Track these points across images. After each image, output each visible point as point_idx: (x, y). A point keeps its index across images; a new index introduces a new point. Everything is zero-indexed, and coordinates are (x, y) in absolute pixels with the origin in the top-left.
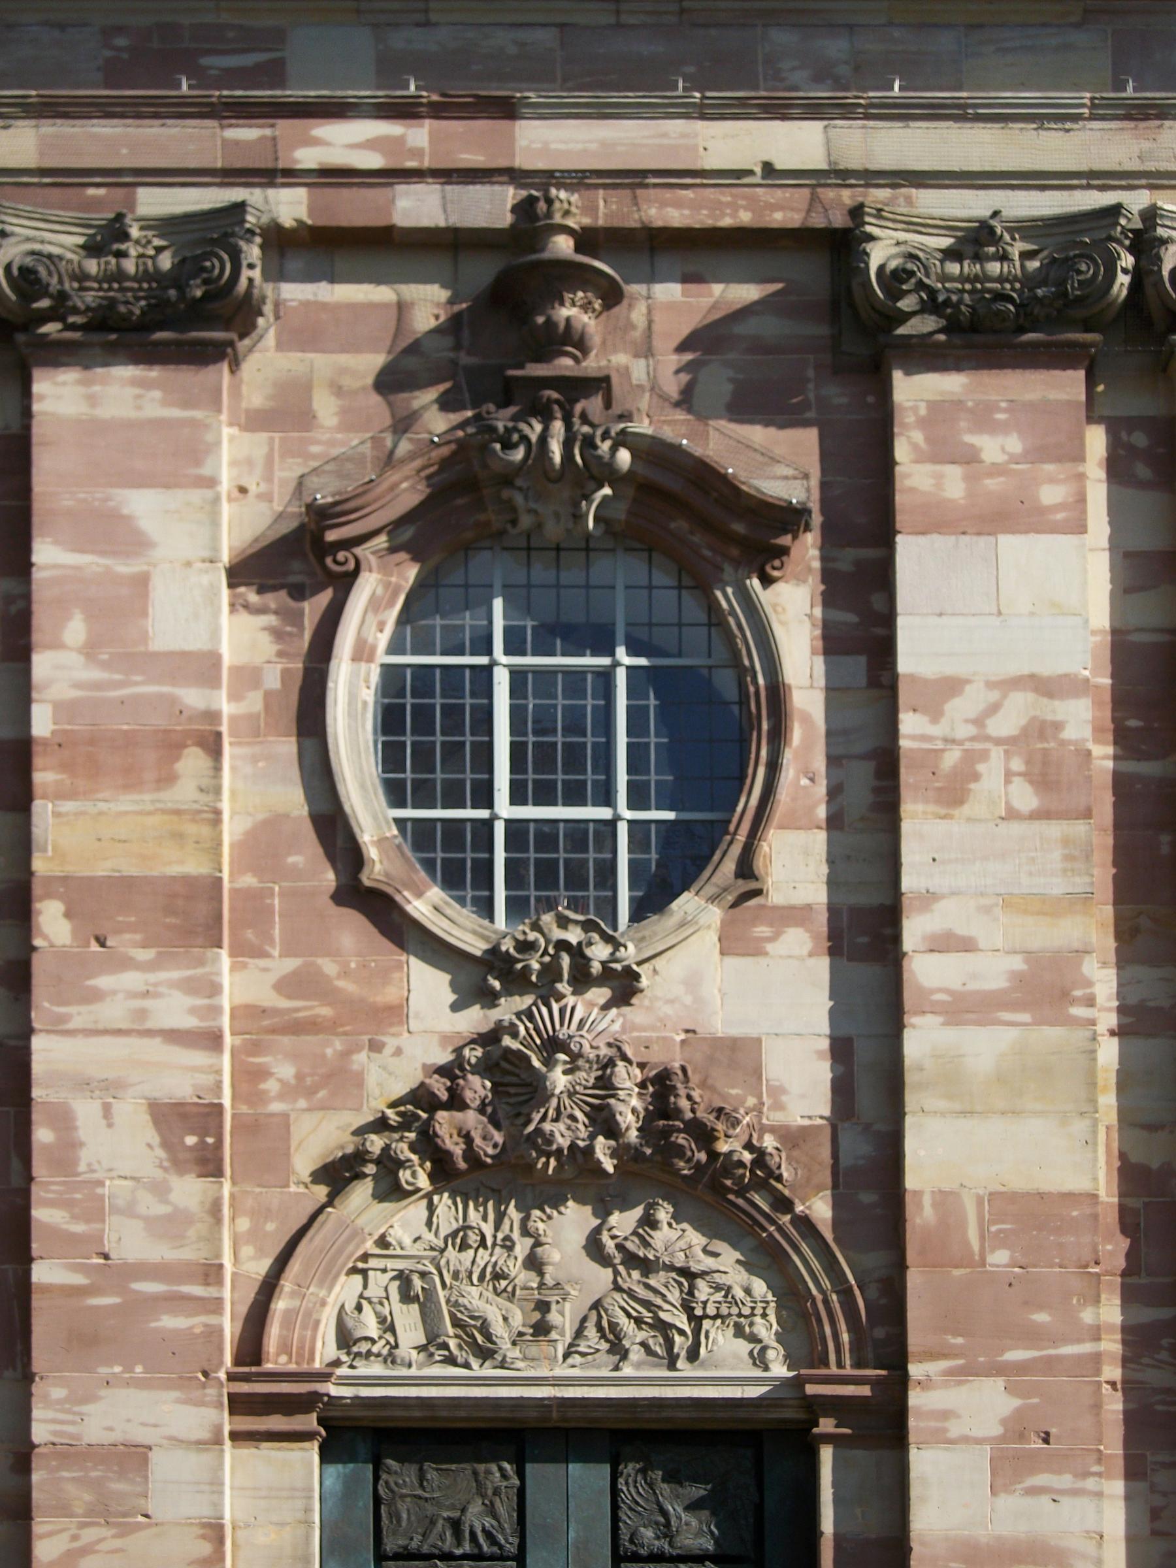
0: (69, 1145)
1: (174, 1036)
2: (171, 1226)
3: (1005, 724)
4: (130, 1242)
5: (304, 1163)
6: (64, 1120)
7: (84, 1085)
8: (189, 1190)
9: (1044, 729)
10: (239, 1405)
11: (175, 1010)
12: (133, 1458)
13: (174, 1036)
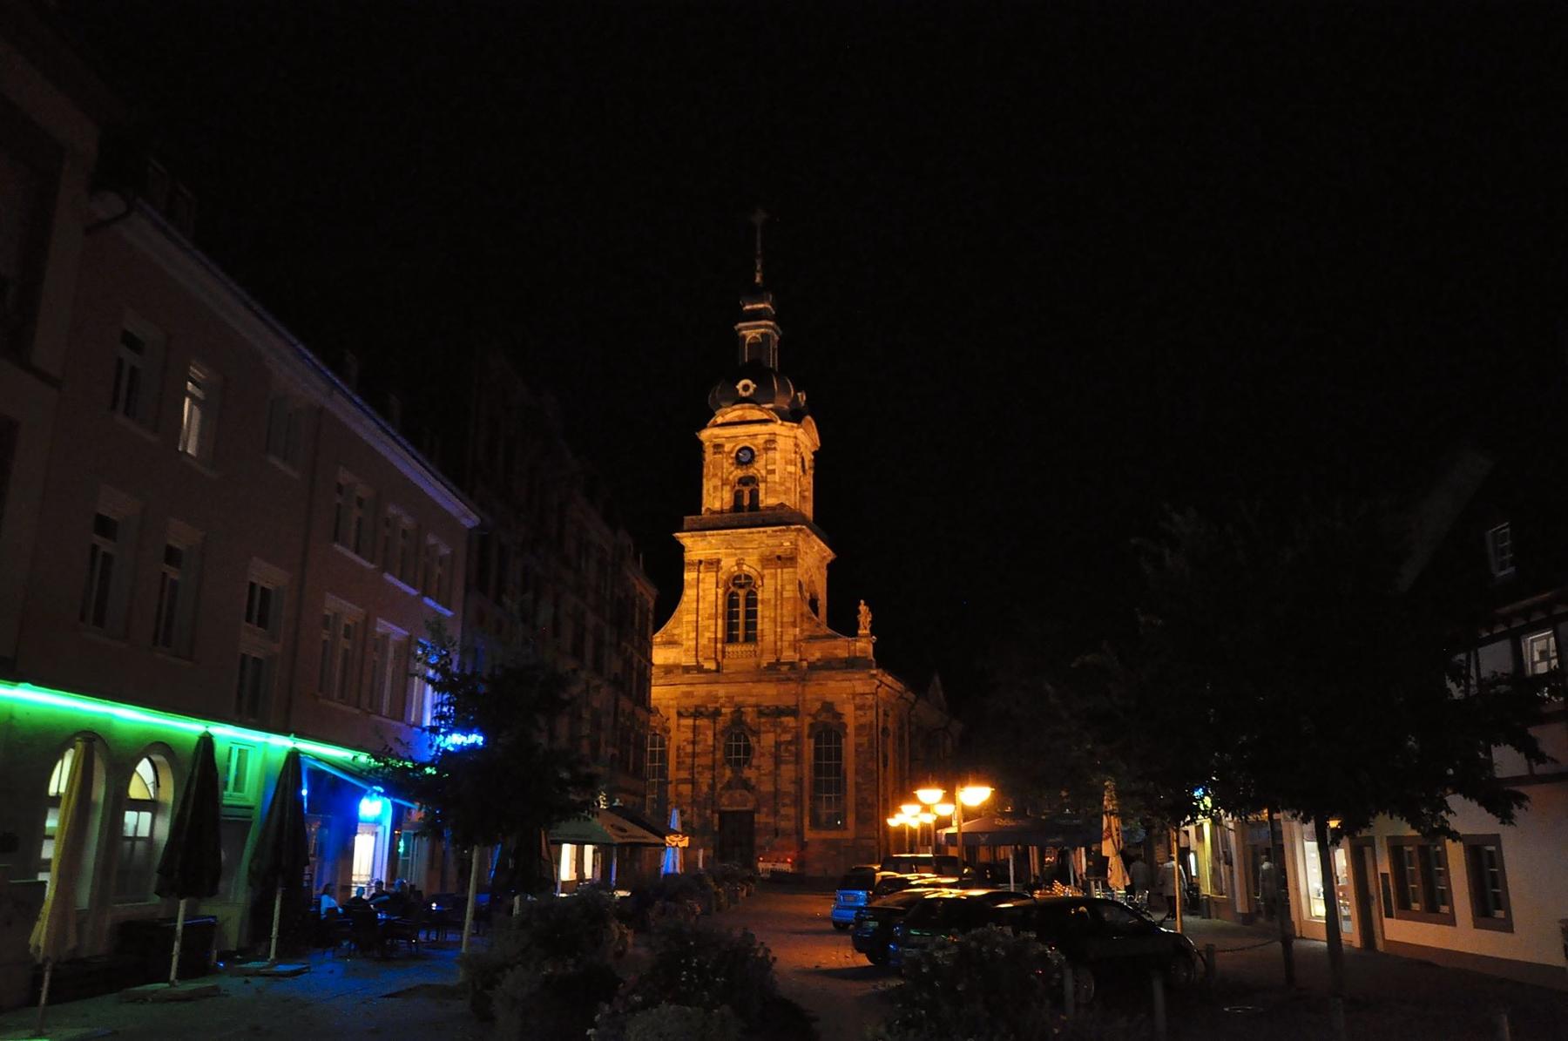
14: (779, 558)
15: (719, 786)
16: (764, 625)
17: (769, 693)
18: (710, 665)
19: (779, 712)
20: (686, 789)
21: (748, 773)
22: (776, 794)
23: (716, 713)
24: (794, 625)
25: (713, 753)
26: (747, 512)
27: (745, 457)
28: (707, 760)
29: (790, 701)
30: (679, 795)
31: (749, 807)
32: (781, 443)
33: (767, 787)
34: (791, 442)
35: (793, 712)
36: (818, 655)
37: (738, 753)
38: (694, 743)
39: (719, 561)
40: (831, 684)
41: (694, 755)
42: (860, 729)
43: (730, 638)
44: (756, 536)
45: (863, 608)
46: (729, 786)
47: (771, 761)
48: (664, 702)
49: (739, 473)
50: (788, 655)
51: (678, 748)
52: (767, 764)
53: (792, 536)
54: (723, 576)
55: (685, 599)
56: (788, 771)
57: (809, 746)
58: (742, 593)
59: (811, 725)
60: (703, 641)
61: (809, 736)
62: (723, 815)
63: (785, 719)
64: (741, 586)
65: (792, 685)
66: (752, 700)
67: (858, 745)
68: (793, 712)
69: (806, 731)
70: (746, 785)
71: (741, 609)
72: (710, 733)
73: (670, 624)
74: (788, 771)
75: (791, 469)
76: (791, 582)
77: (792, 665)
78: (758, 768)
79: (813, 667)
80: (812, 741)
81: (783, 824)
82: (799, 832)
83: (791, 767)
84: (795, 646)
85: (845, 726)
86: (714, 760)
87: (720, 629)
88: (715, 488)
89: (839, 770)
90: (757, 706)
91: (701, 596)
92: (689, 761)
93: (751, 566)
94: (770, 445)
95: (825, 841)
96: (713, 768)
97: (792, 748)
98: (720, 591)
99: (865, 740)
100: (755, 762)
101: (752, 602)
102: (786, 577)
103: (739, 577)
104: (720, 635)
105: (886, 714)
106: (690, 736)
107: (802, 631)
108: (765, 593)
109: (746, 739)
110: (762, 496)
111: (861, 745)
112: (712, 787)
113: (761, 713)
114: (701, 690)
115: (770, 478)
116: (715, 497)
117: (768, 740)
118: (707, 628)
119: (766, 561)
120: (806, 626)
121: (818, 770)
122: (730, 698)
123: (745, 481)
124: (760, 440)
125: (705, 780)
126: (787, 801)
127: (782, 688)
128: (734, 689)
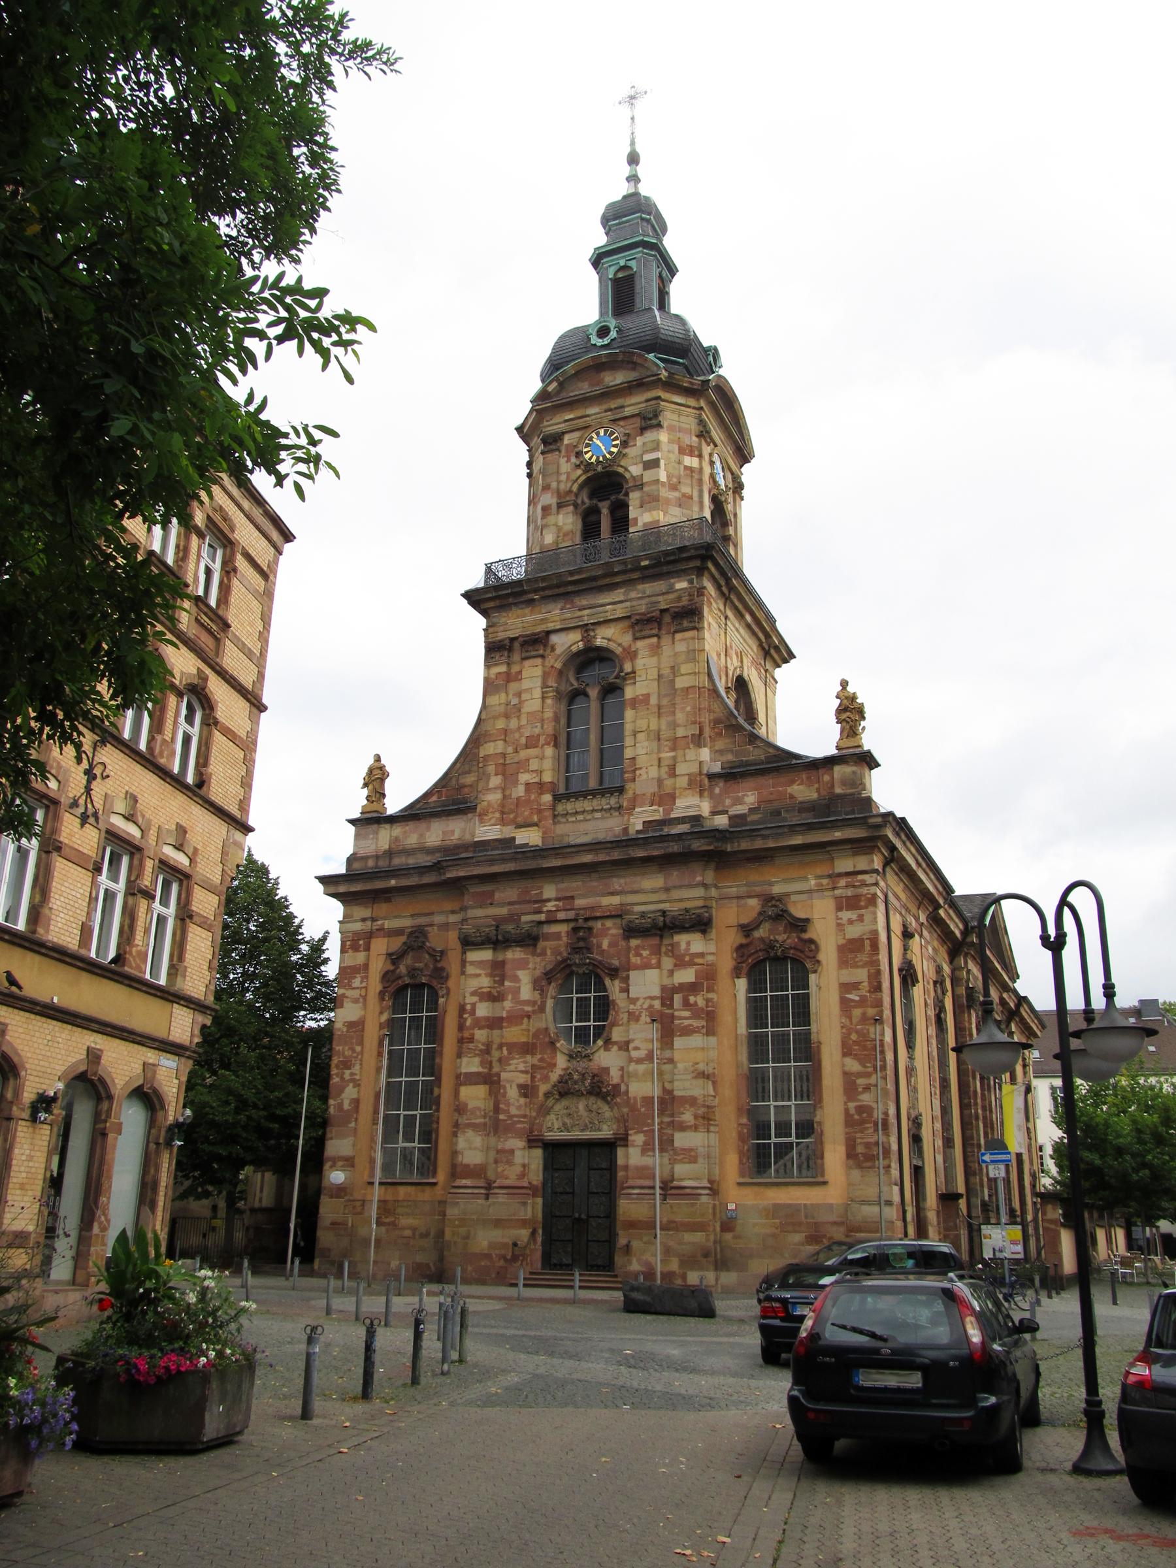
0: (505, 1093)
1: (522, 1072)
2: (519, 1108)
3: (645, 1006)
4: (513, 1111)
5: (541, 1094)
6: (505, 1087)
7: (508, 1081)
8: (522, 1100)
9: (651, 1006)
10: (529, 1141)
11: (521, 1067)
12: (512, 1152)
13: (522, 1072)
20: (475, 1096)
21: (607, 1059)
22: (669, 1101)
31: (606, 1132)
35: (701, 924)
36: (751, 799)
46: (565, 1090)
47: (654, 1031)
51: (462, 1009)
52: (643, 1035)
57: (737, 993)
61: (737, 972)
63: (682, 939)
67: (846, 987)
69: (726, 963)
70: (600, 1089)
78: (625, 1046)
80: (742, 984)
81: (687, 1174)
82: (714, 1190)
88: (546, 509)
89: (808, 1050)
95: (776, 1210)
97: (699, 1000)
99: (861, 975)
100: (617, 1034)
105: (907, 935)
109: (601, 986)
110: (633, 513)
111: (854, 986)
112: (527, 1091)
113: (631, 931)
115: (648, 476)
121: (757, 1047)
125: (514, 1074)
126: (688, 1117)
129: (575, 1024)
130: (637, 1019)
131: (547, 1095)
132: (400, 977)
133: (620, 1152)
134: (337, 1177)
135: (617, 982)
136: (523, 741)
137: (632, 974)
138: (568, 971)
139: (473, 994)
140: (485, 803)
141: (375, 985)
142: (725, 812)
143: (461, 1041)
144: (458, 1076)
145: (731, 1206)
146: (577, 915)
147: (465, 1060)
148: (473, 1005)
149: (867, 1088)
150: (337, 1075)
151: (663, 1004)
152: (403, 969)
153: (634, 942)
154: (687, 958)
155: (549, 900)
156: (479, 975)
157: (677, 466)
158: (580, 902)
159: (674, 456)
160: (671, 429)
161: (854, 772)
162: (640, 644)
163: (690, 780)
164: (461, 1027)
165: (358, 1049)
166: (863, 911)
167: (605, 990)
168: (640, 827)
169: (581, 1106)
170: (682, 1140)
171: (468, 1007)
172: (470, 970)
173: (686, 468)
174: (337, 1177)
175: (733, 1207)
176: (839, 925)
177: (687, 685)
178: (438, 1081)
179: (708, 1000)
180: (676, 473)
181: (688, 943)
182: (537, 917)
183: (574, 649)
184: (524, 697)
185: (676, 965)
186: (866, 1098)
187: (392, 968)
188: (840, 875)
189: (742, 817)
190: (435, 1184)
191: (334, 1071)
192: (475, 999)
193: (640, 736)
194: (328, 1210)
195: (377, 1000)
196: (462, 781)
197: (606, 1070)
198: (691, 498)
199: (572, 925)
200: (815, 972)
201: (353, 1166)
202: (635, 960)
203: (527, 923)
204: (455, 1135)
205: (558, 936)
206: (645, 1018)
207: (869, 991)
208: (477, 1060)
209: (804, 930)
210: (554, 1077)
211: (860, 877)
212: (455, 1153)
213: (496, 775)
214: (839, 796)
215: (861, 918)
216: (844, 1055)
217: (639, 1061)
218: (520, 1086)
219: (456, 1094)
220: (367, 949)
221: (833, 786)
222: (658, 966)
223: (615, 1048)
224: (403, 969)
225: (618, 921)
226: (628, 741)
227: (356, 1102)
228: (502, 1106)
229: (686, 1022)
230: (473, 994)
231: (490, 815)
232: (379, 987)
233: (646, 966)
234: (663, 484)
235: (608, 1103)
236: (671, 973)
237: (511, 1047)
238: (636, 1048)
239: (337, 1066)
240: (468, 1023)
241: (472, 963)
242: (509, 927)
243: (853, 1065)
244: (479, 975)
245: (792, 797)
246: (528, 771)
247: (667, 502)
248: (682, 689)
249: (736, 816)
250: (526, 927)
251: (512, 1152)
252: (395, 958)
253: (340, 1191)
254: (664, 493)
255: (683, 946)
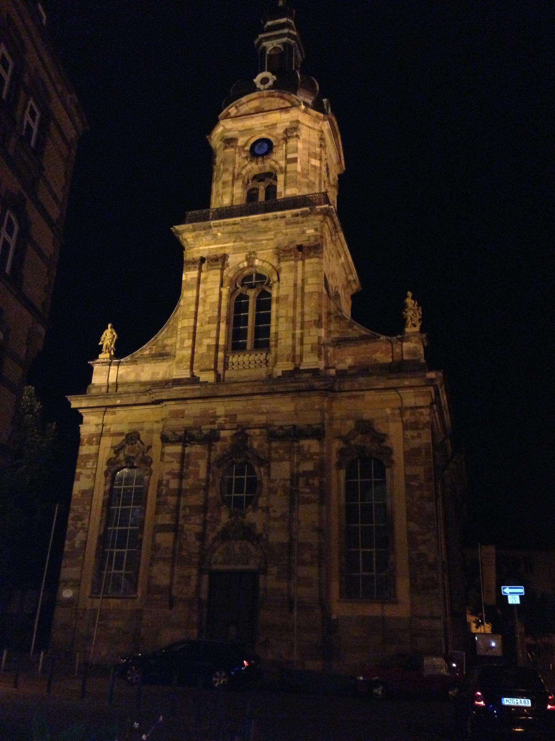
9: (284, 485)
11: (198, 521)
14: (300, 248)
15: (211, 536)
16: (280, 326)
17: (283, 409)
18: (208, 377)
19: (295, 434)
20: (165, 539)
23: (211, 438)
24: (318, 324)
25: (206, 489)
26: (262, 198)
27: (262, 148)
28: (196, 500)
29: (311, 418)
30: (155, 547)
31: (252, 566)
32: (304, 132)
33: (278, 537)
34: (314, 137)
36: (349, 361)
37: (239, 489)
38: (181, 476)
39: (224, 257)
40: (370, 396)
41: (179, 492)
42: (411, 455)
43: (236, 344)
44: (271, 224)
45: (409, 301)
48: (147, 426)
49: (254, 167)
50: (310, 361)
51: (160, 484)
52: (279, 503)
53: (317, 220)
54: (229, 273)
55: (182, 303)
56: (308, 514)
57: (338, 478)
58: (252, 294)
59: (341, 452)
60: (201, 350)
61: (339, 466)
62: (214, 575)
63: (305, 443)
64: (251, 287)
65: (316, 399)
66: (263, 419)
67: (409, 478)
68: (317, 433)
69: (334, 459)
71: (251, 314)
72: (203, 464)
73: (162, 334)
74: (308, 514)
75: (315, 162)
76: (315, 274)
77: (315, 372)
78: (267, 510)
79: (342, 374)
80: (343, 473)
82: (324, 604)
83: (314, 507)
84: (319, 349)
85: (389, 451)
86: (207, 501)
87: (222, 334)
90: (266, 426)
91: (202, 297)
92: (172, 500)
93: (264, 261)
94: (291, 132)
96: (204, 509)
98: (225, 291)
99: (419, 470)
100: (262, 502)
101: (264, 303)
102: (308, 268)
103: (249, 277)
104: (222, 342)
106: (176, 466)
107: (329, 333)
108: (281, 289)
109: (252, 471)
110: (280, 188)
111: (415, 477)
112: (202, 537)
114: (194, 408)
115: (290, 167)
116: (226, 192)
117: (281, 470)
118: (206, 334)
119: (282, 253)
120: (333, 327)
121: (350, 513)
122: (231, 417)
123: (259, 178)
124: (280, 131)
125: (192, 526)
126: (307, 557)
127: (302, 402)
128: (236, 405)
129: (233, 495)
130: (275, 493)
131: (215, 539)
132: (119, 462)
133: (261, 578)
134: (67, 594)
135: (262, 469)
136: (207, 319)
137: (273, 464)
138: (230, 461)
139: (167, 474)
140: (181, 356)
141: (102, 466)
142: (334, 367)
143: (158, 504)
144: (155, 527)
145: (334, 617)
146: (238, 426)
147: (160, 517)
148: (168, 481)
149: (424, 542)
150: (72, 525)
151: (292, 484)
152: (121, 456)
153: (274, 445)
154: (308, 456)
155: (220, 417)
156: (172, 462)
157: (307, 164)
158: (240, 418)
159: (306, 158)
160: (304, 141)
161: (416, 347)
162: (283, 265)
163: (312, 347)
164: (159, 495)
165: (88, 508)
166: (421, 432)
167: (254, 473)
168: (280, 374)
169: (237, 548)
170: (303, 571)
171: (165, 482)
172: (167, 458)
173: (312, 165)
174: (67, 594)
175: (336, 617)
176: (405, 439)
177: (312, 290)
178: (141, 530)
179: (321, 483)
180: (306, 167)
181: (309, 446)
182: (212, 426)
183: (241, 266)
184: (208, 293)
185: (301, 460)
186: (423, 548)
187: (114, 456)
188: (406, 408)
189: (345, 371)
190: (135, 598)
191: (70, 522)
192: (169, 477)
193: (281, 320)
194: (60, 615)
195: (103, 477)
196: (166, 342)
197: (254, 525)
198: (314, 183)
199: (234, 432)
200: (390, 467)
201: (79, 585)
202: (274, 456)
203: (206, 429)
204: (151, 565)
205: (225, 439)
206: (280, 492)
207: (424, 481)
208: (168, 516)
209: (383, 441)
210: (219, 528)
211: (419, 410)
212: (150, 578)
213: (189, 339)
214: (407, 361)
215: (419, 436)
216: (408, 520)
217: (275, 519)
218: (197, 534)
219: (154, 537)
220: (99, 443)
221: (402, 355)
222: (290, 460)
223: (260, 511)
224: (121, 456)
225: (264, 431)
226: (273, 322)
227: (85, 543)
228: (184, 546)
229: (306, 496)
230: (169, 473)
231: (184, 363)
232: (105, 468)
233: (282, 460)
234: (299, 173)
235: (254, 545)
236: (298, 464)
237: (192, 508)
238: (274, 511)
239: (72, 519)
240: (164, 492)
241: (168, 454)
242: (195, 432)
243: (414, 527)
244: (172, 462)
245: (375, 360)
246: (209, 338)
247: (301, 183)
248: (309, 293)
249: (341, 371)
250: (205, 432)
251: (189, 577)
252: (117, 450)
253: (70, 602)
254: (299, 177)
255: (306, 448)
